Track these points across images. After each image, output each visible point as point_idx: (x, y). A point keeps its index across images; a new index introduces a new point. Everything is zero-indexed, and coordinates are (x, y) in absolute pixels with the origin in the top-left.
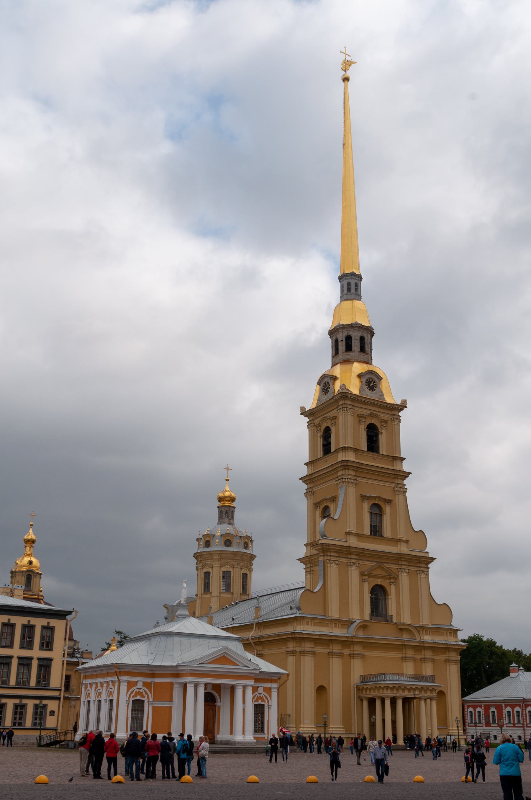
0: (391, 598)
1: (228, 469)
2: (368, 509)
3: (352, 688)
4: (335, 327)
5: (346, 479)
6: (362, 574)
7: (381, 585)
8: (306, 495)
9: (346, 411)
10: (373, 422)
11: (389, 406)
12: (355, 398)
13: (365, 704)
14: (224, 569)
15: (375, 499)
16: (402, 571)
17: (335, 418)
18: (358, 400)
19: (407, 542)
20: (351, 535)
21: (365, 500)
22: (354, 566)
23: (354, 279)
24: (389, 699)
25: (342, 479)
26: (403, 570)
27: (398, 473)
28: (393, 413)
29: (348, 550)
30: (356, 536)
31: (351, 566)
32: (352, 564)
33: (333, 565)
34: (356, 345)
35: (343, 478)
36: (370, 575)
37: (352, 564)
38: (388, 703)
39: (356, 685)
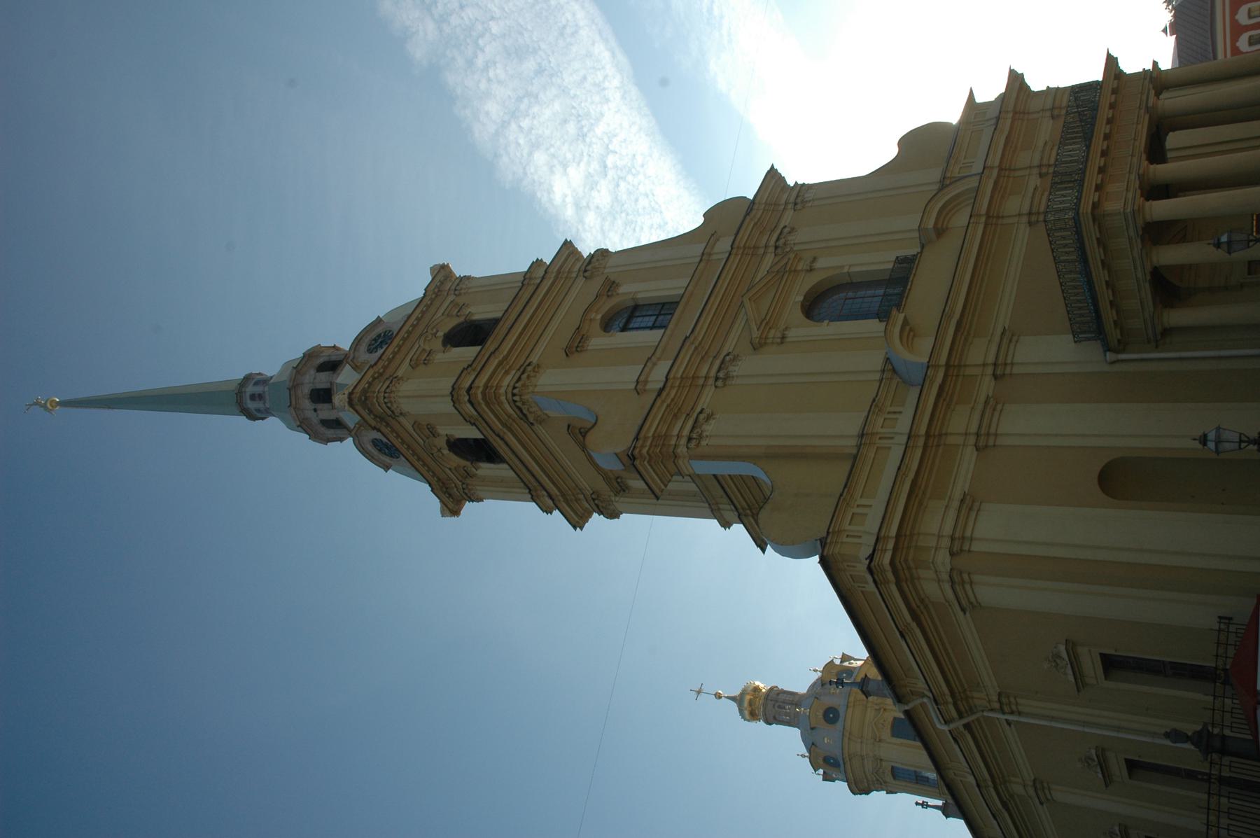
0: (850, 266)
1: (699, 692)
3: (1117, 368)
4: (298, 426)
5: (516, 391)
8: (613, 515)
9: (392, 395)
10: (441, 334)
11: (427, 301)
12: (375, 373)
13: (1177, 317)
14: (886, 733)
15: (591, 320)
16: (785, 244)
17: (416, 425)
20: (648, 376)
21: (581, 344)
22: (731, 368)
24: (1148, 204)
25: (519, 404)
26: (781, 242)
28: (446, 294)
30: (655, 364)
31: (727, 377)
32: (721, 375)
33: (709, 428)
34: (322, 380)
35: (515, 401)
37: (721, 375)
38: (1162, 209)
39: (1110, 356)
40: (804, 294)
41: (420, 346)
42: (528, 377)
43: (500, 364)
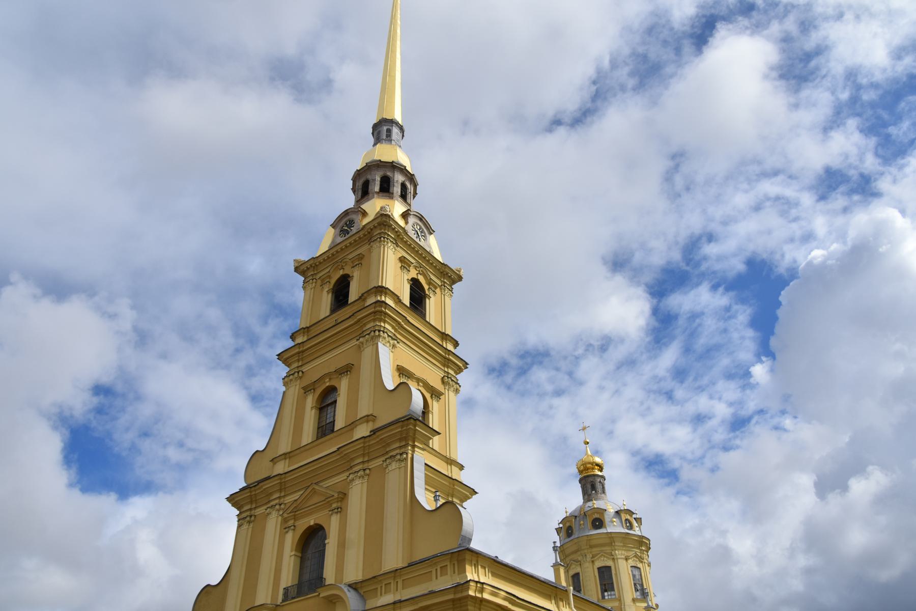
2: (312, 405)
6: (285, 521)
7: (316, 524)
10: (341, 272)
12: (312, 264)
15: (324, 382)
18: (320, 263)
19: (369, 418)
22: (274, 512)
23: (376, 130)
27: (358, 318)
29: (262, 490)
30: (285, 459)
36: (295, 515)
40: (316, 523)
41: (329, 272)
42: (291, 380)
43: (299, 353)
